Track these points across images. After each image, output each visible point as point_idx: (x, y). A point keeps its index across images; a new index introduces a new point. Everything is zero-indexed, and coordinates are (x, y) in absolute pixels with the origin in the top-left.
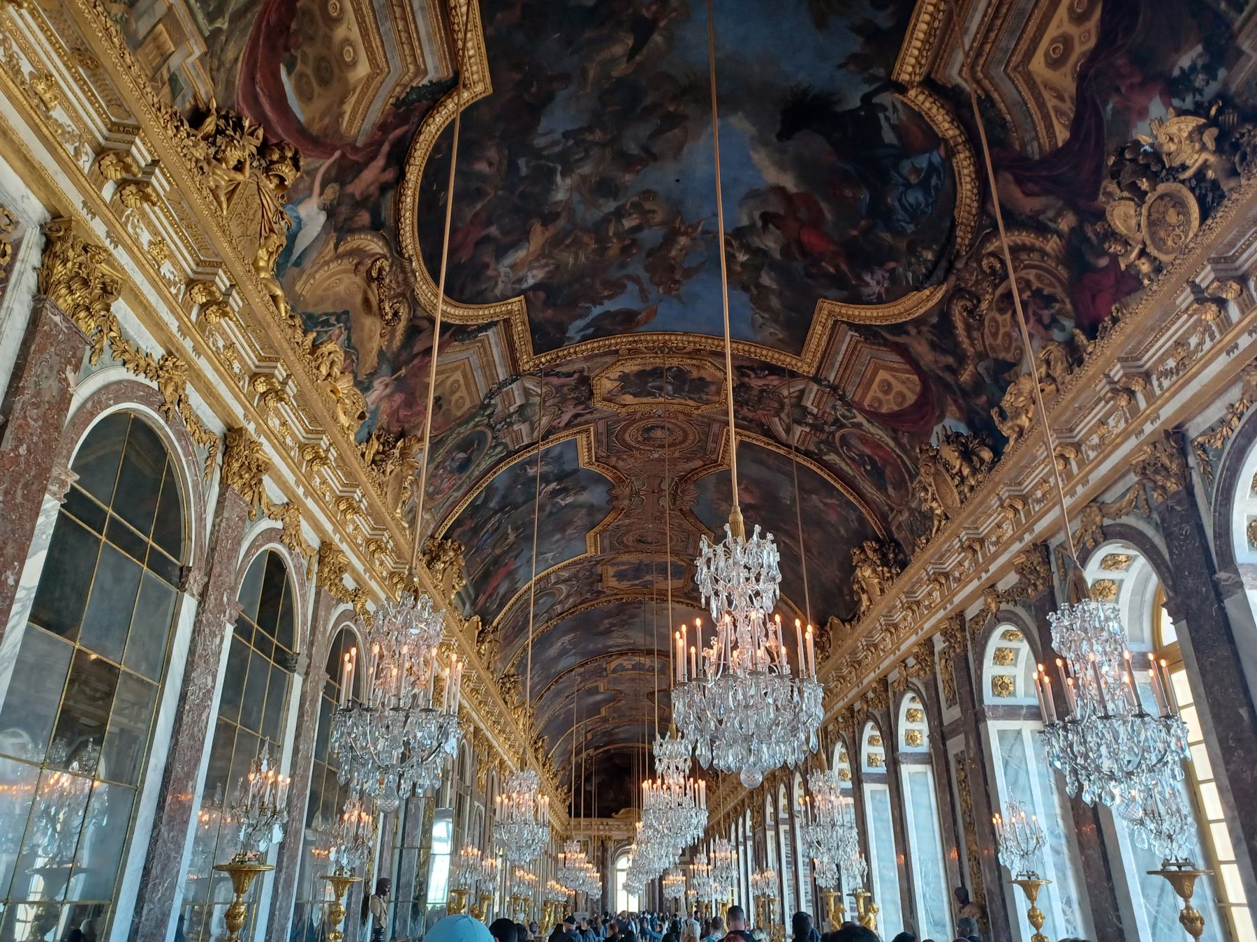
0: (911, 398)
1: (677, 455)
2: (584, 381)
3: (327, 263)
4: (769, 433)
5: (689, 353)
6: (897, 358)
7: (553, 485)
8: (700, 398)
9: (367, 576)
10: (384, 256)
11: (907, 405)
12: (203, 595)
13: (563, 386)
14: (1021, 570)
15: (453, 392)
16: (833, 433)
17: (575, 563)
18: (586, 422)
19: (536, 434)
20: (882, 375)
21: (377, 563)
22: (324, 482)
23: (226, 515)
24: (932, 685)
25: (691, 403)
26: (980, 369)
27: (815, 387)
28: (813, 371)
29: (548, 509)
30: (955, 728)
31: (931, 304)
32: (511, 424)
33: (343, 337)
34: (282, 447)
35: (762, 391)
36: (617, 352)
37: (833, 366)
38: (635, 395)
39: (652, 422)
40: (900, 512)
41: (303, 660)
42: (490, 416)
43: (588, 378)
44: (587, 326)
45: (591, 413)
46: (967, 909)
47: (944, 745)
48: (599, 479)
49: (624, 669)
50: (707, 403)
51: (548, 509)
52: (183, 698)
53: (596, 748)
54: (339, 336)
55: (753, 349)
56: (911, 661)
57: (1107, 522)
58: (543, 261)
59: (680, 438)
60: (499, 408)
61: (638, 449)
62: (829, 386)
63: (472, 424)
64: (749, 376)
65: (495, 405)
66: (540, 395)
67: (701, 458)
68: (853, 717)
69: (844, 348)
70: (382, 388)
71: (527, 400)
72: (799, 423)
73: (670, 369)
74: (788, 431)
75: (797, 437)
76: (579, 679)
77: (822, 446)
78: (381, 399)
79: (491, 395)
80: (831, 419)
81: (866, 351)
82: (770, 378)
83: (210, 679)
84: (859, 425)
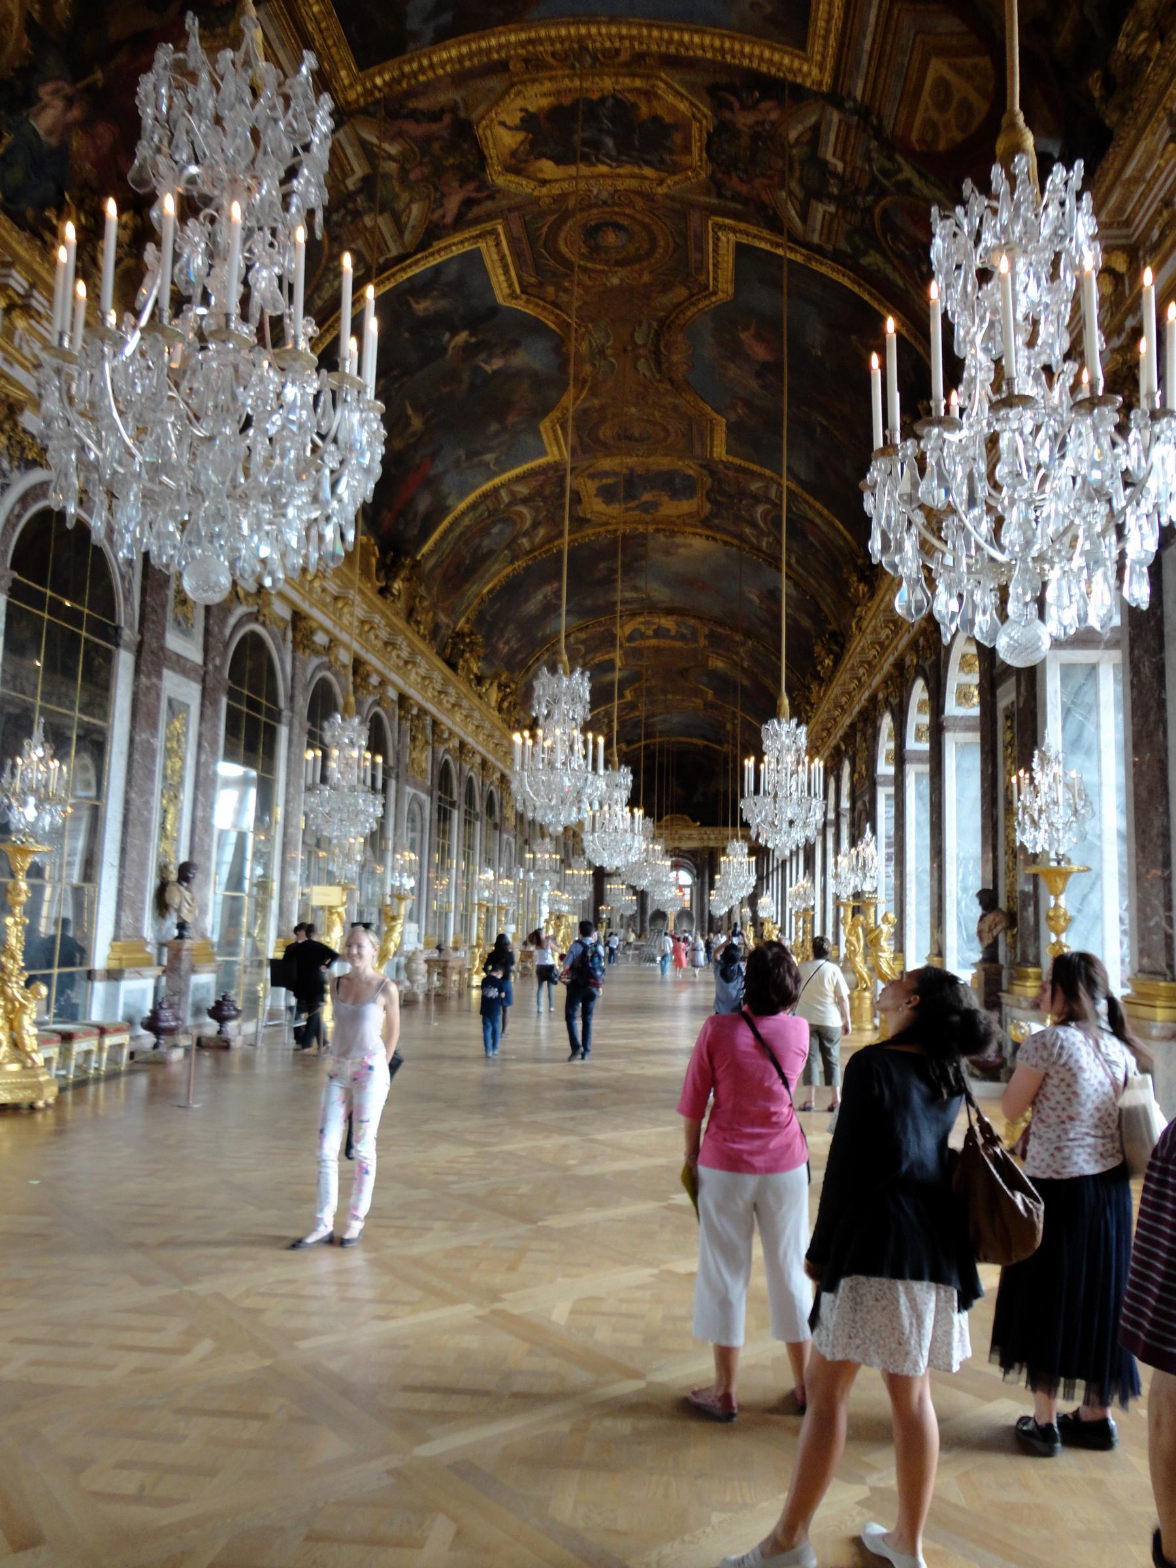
1: (646, 278)
2: (464, 132)
4: (774, 222)
5: (626, 64)
7: (463, 336)
8: (662, 161)
13: (428, 139)
16: (869, 211)
17: (532, 473)
18: (490, 217)
19: (407, 236)
20: (937, 68)
25: (648, 172)
28: (827, 79)
29: (466, 377)
32: (357, 214)
35: (756, 137)
36: (502, 67)
37: (858, 62)
38: (559, 161)
45: (491, 197)
46: (990, 917)
47: (993, 695)
48: (534, 327)
49: (643, 636)
50: (674, 169)
51: (466, 377)
55: (727, 45)
59: (646, 246)
61: (585, 270)
64: (732, 110)
66: (391, 158)
68: (901, 675)
69: (872, 20)
70: (59, 104)
71: (374, 166)
73: (603, 100)
74: (804, 216)
76: (582, 648)
77: (857, 239)
78: (68, 128)
80: (865, 183)
82: (766, 105)
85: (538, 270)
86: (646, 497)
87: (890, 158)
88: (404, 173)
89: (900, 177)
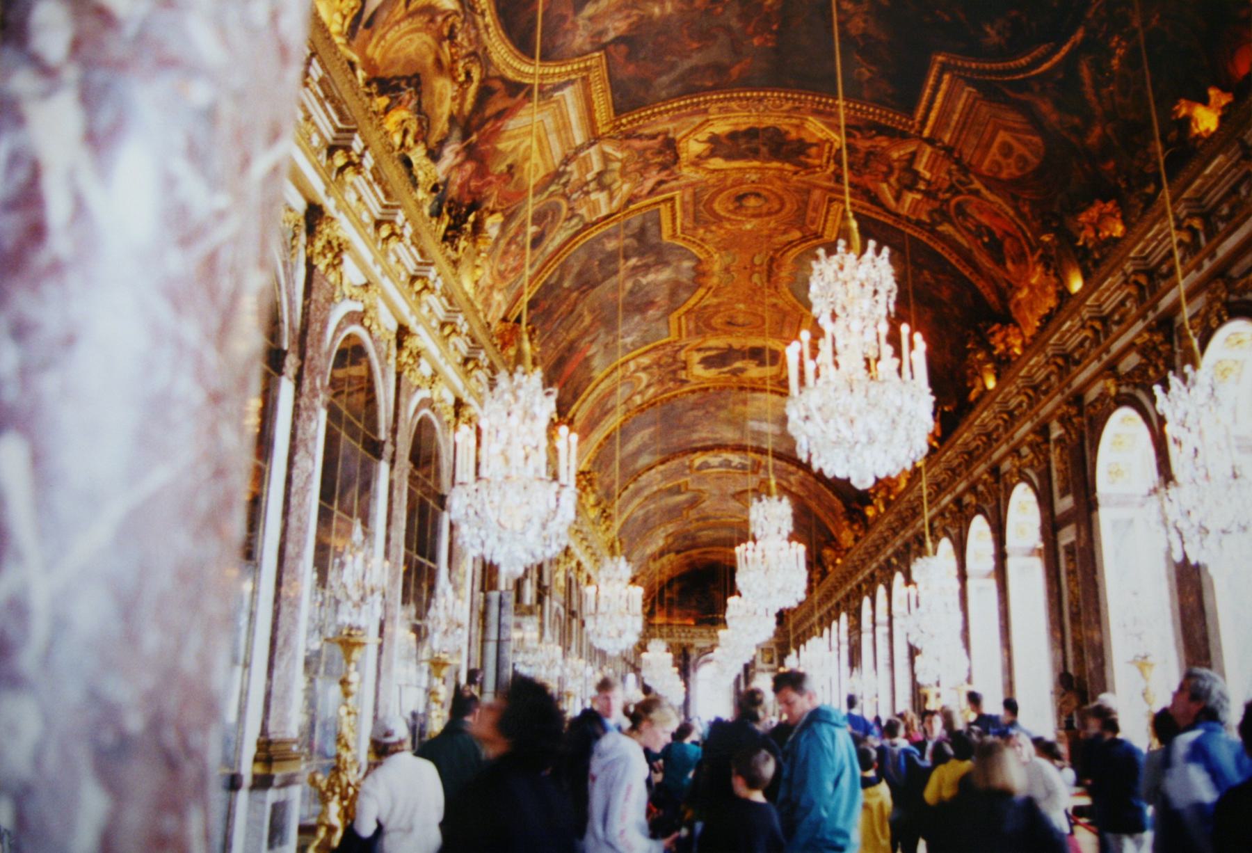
0: (1034, 160)
2: (670, 146)
3: (398, 23)
6: (1019, 118)
7: (633, 261)
9: (442, 362)
10: (456, 13)
11: (1029, 169)
12: (298, 380)
13: (645, 149)
14: (1143, 351)
15: (527, 159)
16: (947, 201)
18: (672, 190)
20: (1002, 136)
21: (452, 347)
22: (399, 261)
23: (314, 296)
24: (1046, 476)
26: (1108, 131)
27: (928, 150)
30: (1067, 519)
31: (1056, 58)
32: (588, 193)
33: (414, 102)
34: (359, 224)
39: (745, 188)
40: (1020, 289)
41: (388, 448)
42: (565, 185)
43: (673, 140)
44: (673, 83)
45: (676, 179)
52: (289, 481)
53: (678, 552)
54: (409, 102)
56: (1025, 450)
57: (1233, 298)
58: (625, 13)
60: (575, 176)
61: (729, 220)
62: (940, 148)
63: (546, 194)
65: (571, 173)
67: (800, 229)
69: (960, 106)
72: (911, 188)
74: (898, 198)
75: (907, 205)
77: (935, 216)
78: (452, 168)
79: (567, 160)
80: (946, 185)
81: (984, 110)
82: (878, 138)
83: (310, 462)
84: (977, 193)
85: (696, 219)
86: (738, 364)
87: (965, 175)
88: (624, 167)
89: (972, 187)
